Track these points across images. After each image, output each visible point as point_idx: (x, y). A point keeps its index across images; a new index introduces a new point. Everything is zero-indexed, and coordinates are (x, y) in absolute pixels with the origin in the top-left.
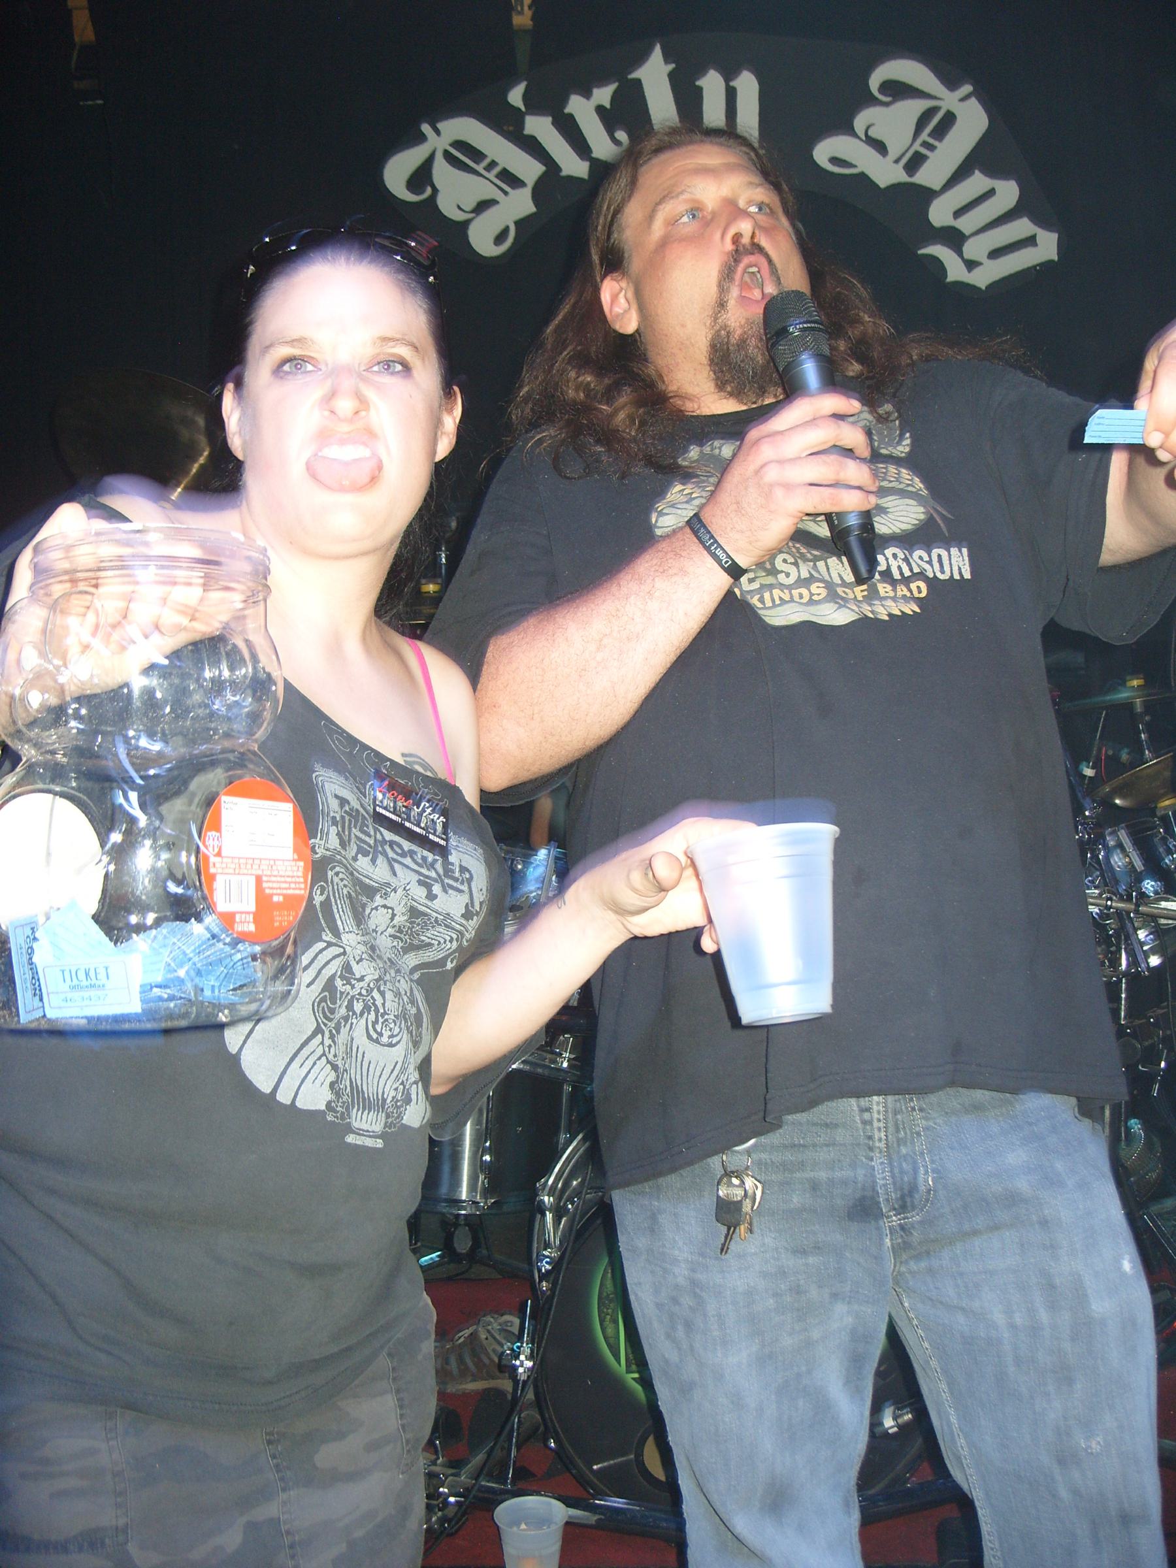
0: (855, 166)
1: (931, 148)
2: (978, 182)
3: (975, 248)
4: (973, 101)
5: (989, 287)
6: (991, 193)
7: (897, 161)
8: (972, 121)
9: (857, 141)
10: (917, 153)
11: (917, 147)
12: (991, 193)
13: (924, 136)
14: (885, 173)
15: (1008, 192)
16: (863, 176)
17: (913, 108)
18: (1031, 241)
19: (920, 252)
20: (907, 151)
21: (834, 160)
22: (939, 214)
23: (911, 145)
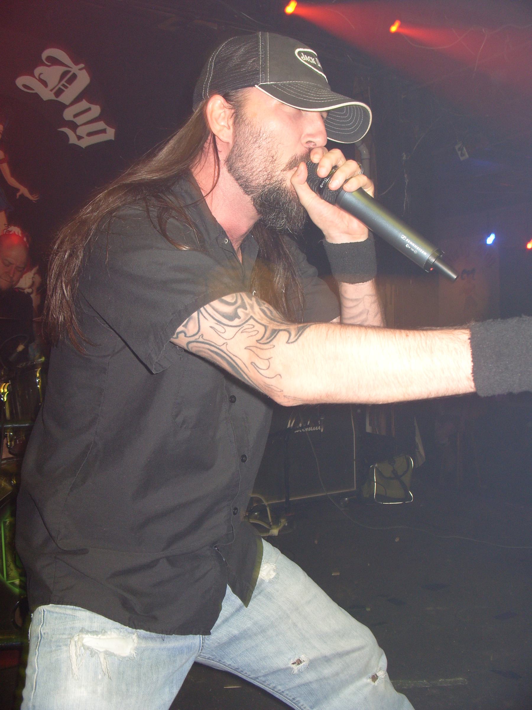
0: (33, 90)
1: (66, 87)
2: (84, 104)
3: (81, 131)
4: (84, 71)
5: (86, 148)
6: (89, 109)
7: (51, 90)
8: (83, 79)
9: (35, 79)
10: (60, 89)
11: (60, 86)
12: (89, 109)
13: (63, 82)
14: (47, 95)
15: (96, 110)
16: (36, 95)
17: (59, 70)
18: (104, 131)
19: (60, 130)
20: (56, 87)
21: (25, 86)
22: (68, 114)
23: (57, 85)
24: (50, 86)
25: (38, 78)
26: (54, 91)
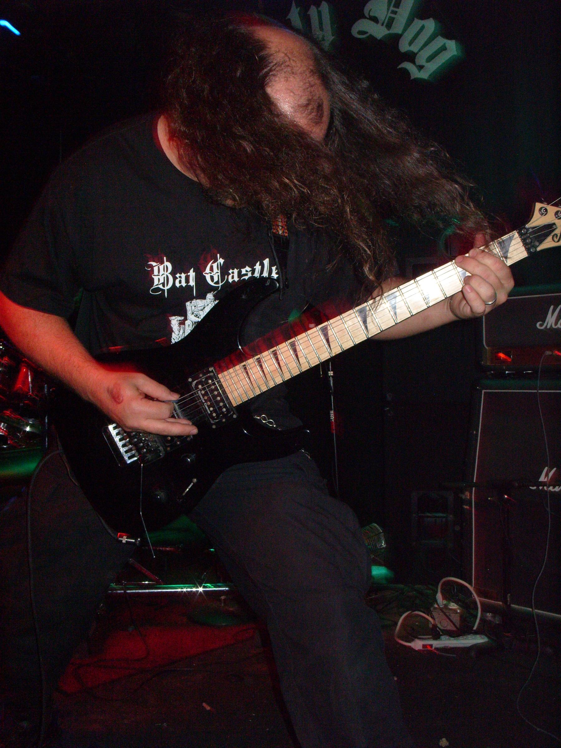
0: (367, 33)
3: (421, 60)
14: (379, 32)
16: (371, 35)
22: (404, 47)
24: (381, 22)
25: (368, 17)
26: (385, 24)
